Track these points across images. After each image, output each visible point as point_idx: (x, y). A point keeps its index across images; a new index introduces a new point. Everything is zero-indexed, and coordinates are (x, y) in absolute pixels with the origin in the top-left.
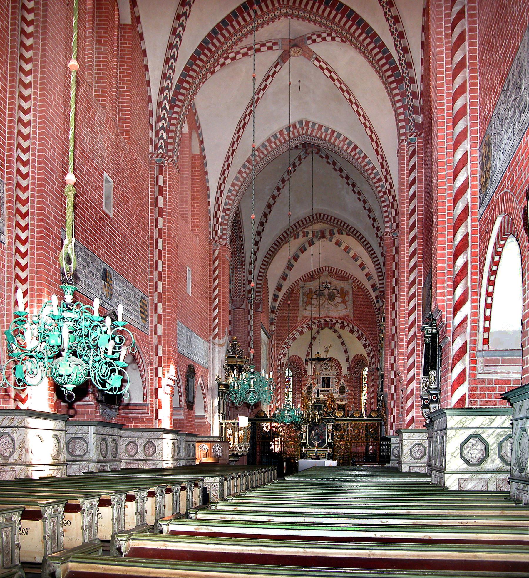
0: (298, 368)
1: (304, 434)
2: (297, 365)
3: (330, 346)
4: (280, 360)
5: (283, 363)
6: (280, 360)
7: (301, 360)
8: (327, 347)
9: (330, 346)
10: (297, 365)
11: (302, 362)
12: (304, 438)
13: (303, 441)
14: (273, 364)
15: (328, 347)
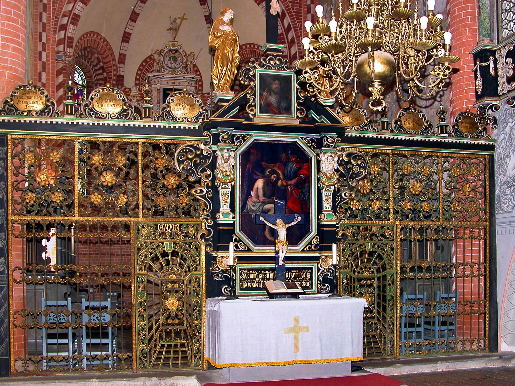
0: (102, 68)
1: (224, 191)
2: (99, 61)
3: (182, 19)
4: (64, 27)
5: (71, 39)
6: (64, 27)
7: (110, 49)
8: (175, 21)
9: (182, 19)
10: (99, 61)
11: (112, 54)
12: (225, 206)
13: (221, 218)
14: (44, 35)
15: (178, 21)
